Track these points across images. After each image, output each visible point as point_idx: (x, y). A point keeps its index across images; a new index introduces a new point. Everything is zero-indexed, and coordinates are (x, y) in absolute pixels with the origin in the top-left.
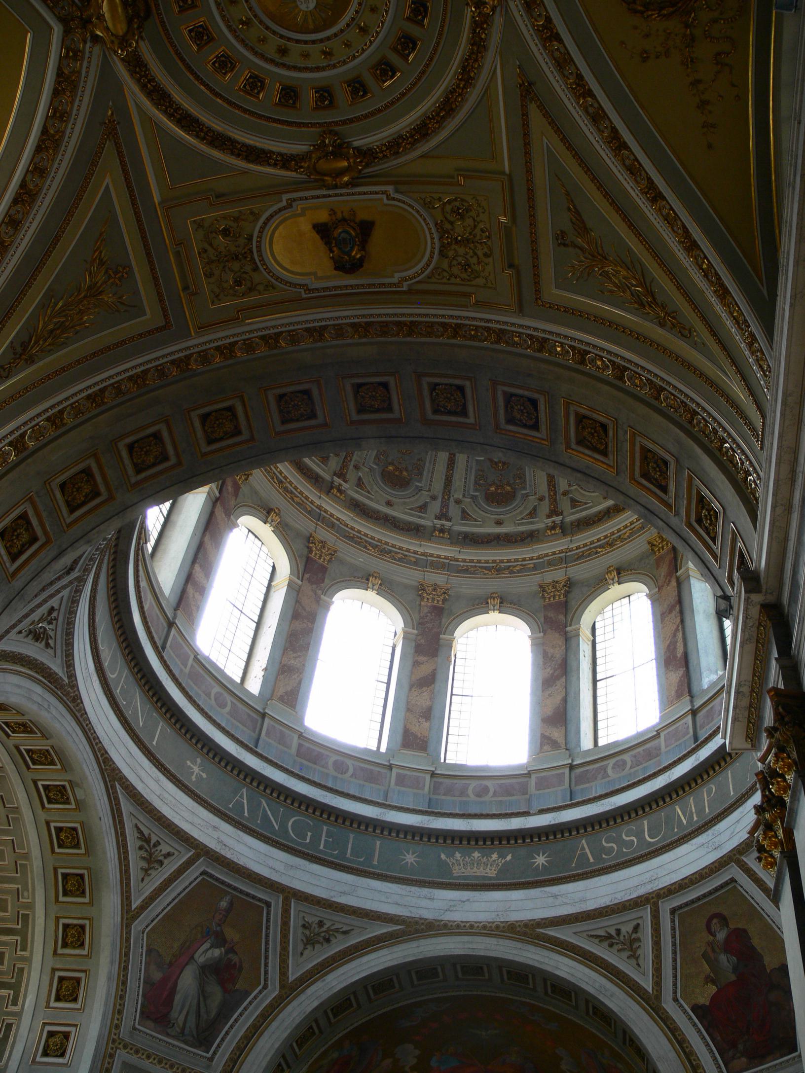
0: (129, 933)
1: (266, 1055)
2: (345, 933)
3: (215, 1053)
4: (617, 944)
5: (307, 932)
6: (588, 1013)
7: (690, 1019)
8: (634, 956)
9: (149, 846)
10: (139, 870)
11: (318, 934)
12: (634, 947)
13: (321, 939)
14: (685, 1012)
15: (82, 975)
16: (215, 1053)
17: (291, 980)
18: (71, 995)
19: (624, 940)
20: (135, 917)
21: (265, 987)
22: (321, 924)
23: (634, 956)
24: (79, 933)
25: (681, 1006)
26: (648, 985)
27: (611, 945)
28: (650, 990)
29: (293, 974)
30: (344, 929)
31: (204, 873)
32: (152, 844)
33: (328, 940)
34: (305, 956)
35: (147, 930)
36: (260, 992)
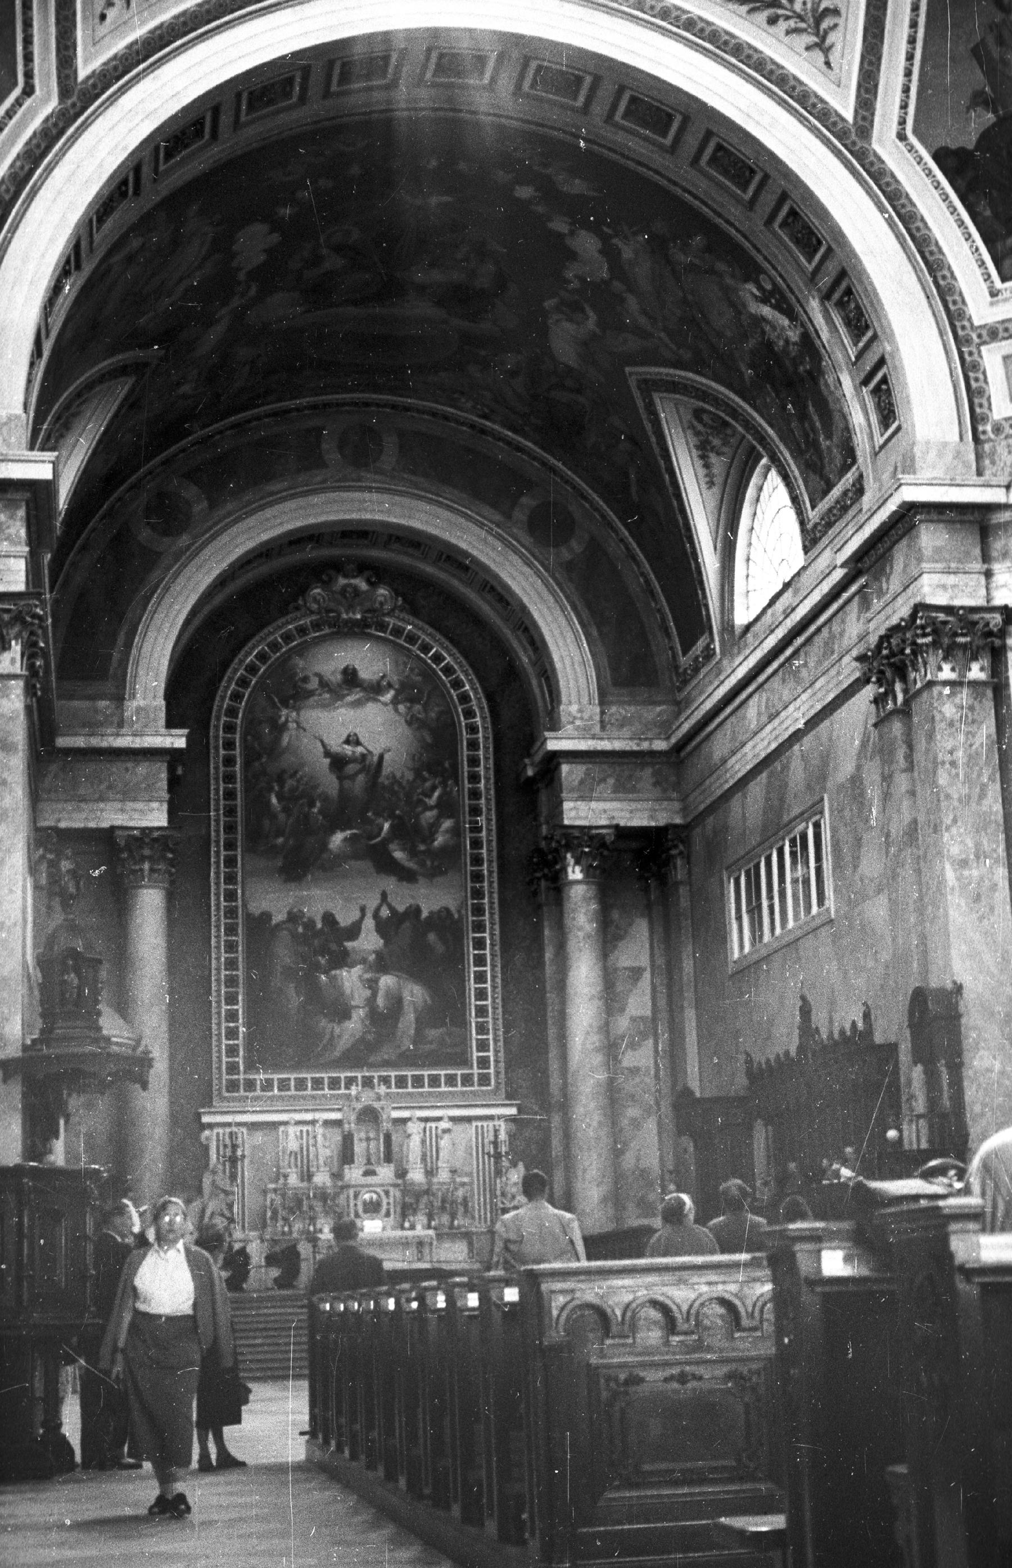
1: (52, 240)
4: (787, 18)
6: (695, 161)
7: (929, 173)
8: (822, 45)
12: (824, 25)
14: (920, 160)
17: (82, 73)
19: (805, 10)
21: (29, 90)
23: (822, 45)
25: (911, 149)
26: (846, 107)
27: (772, 21)
28: (849, 115)
29: (86, 61)
34: (108, 20)
36: (19, 103)
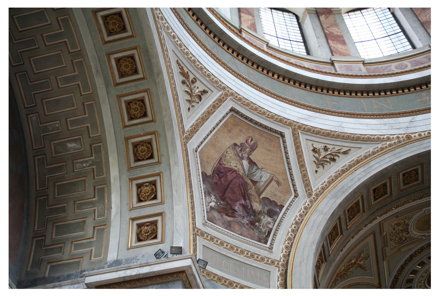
0: (186, 150)
2: (345, 153)
3: (272, 244)
5: (316, 155)
9: (189, 81)
10: (186, 101)
11: (324, 157)
13: (329, 160)
15: (157, 178)
16: (272, 244)
18: (151, 194)
20: (188, 138)
22: (326, 149)
24: (148, 148)
30: (344, 149)
31: (232, 110)
32: (190, 80)
33: (334, 160)
35: (199, 150)
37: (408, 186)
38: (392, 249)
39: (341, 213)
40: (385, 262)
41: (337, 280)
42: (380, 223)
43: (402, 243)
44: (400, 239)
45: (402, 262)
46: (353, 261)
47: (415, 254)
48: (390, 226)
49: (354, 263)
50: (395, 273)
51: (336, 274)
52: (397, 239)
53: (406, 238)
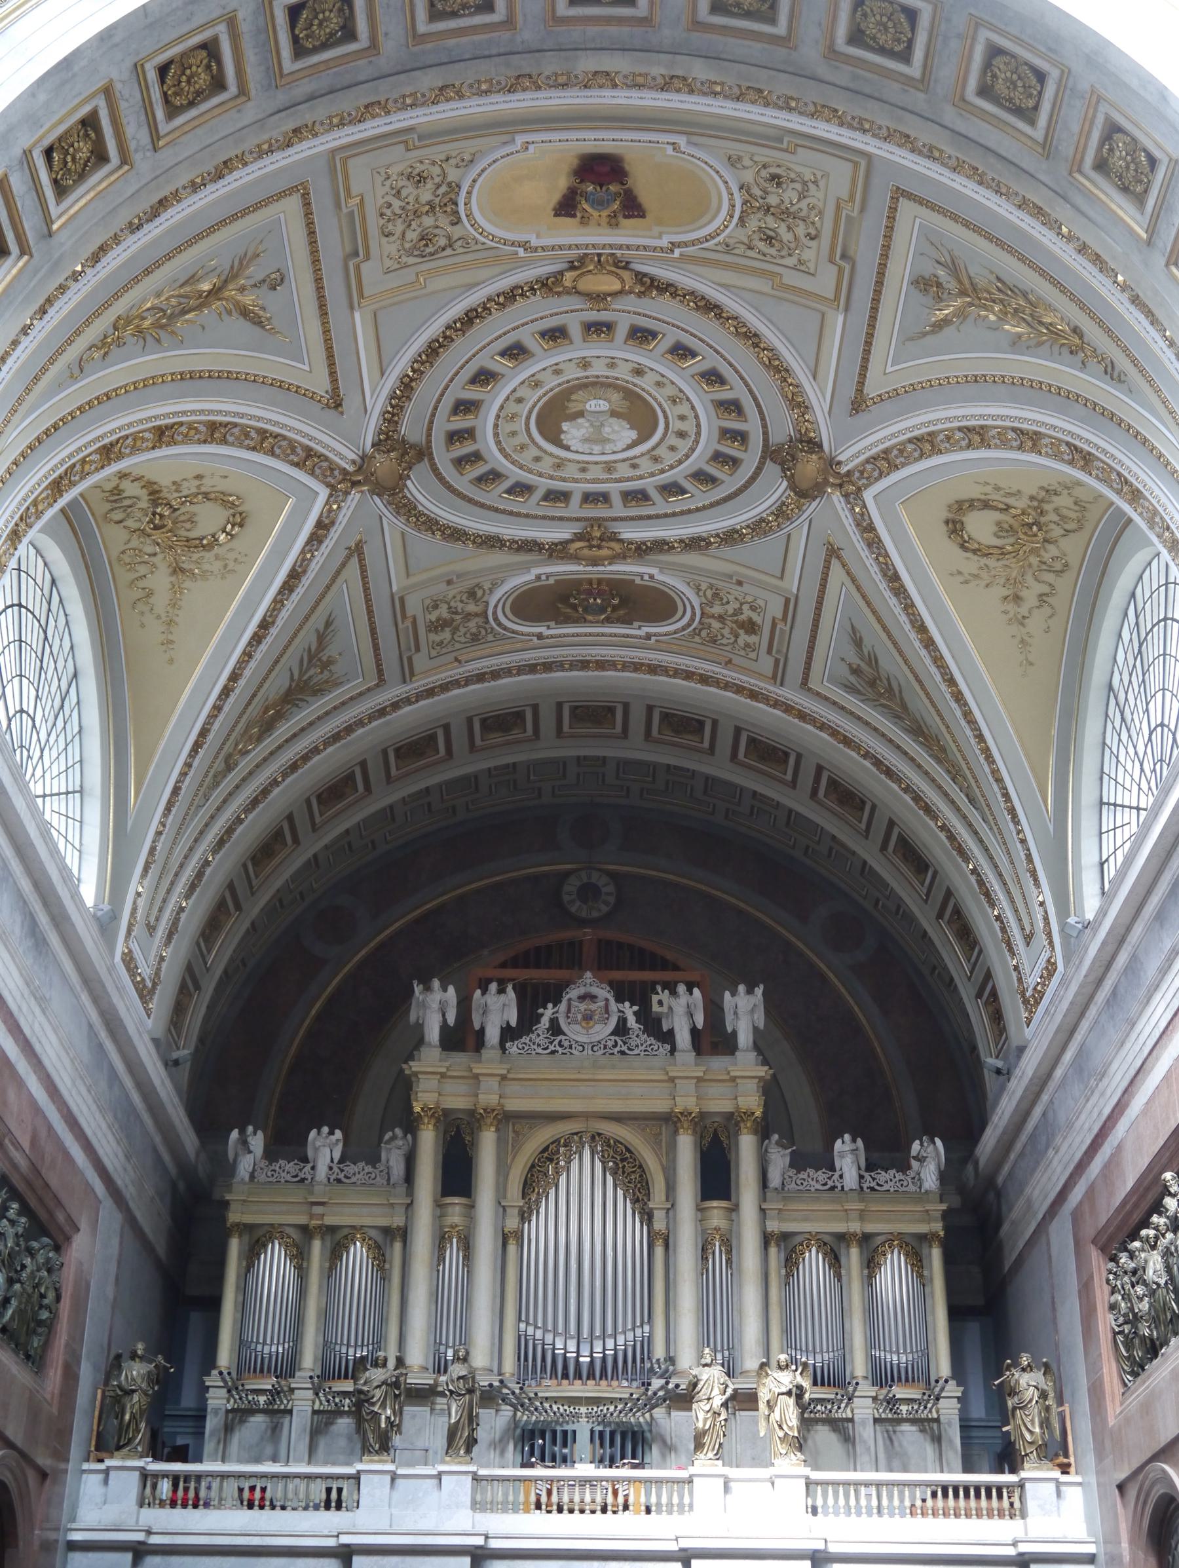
37: (452, 24)
38: (388, 272)
39: (118, 72)
40: (357, 316)
41: (119, 342)
42: (333, 152)
43: (432, 254)
44: (426, 238)
45: (434, 329)
46: (206, 287)
47: (485, 308)
48: (379, 180)
49: (210, 292)
50: (401, 365)
51: (110, 316)
52: (412, 235)
53: (449, 238)
